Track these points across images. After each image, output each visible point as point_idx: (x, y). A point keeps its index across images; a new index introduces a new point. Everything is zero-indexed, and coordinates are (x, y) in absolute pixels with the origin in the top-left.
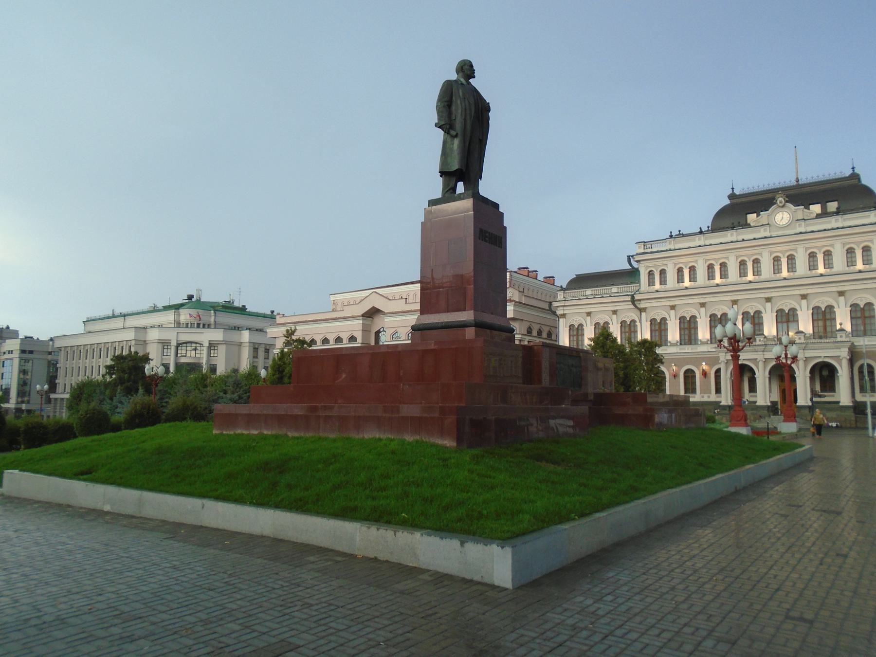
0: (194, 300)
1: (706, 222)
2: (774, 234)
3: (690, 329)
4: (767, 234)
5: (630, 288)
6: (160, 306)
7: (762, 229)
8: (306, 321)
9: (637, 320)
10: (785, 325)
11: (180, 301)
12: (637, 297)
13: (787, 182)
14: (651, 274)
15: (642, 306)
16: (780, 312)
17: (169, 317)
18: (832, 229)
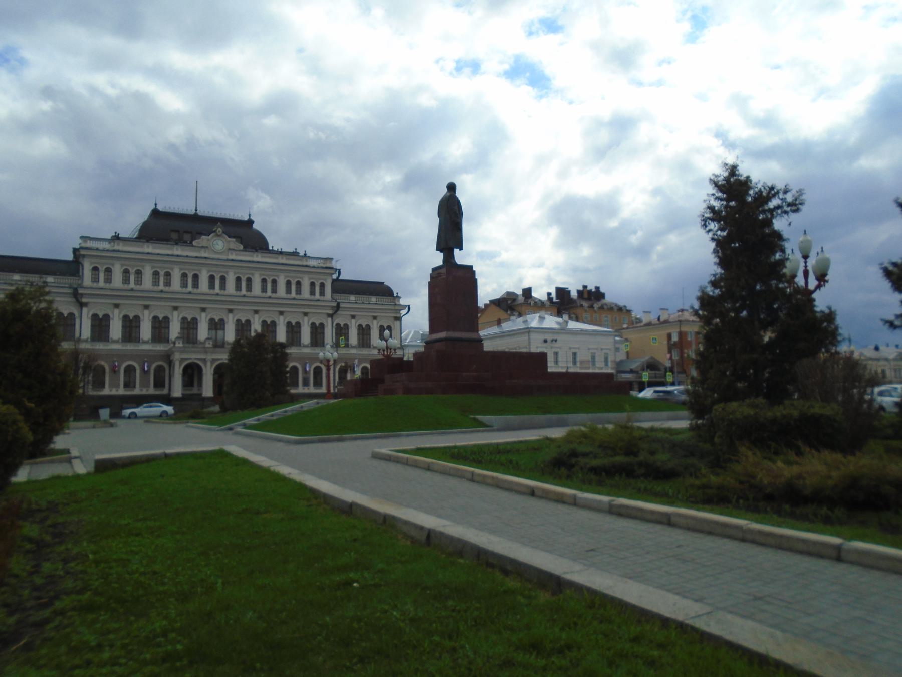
4: (206, 255)
7: (203, 250)
9: (77, 315)
10: (214, 332)
12: (81, 291)
15: (84, 300)
16: (212, 321)
18: (253, 262)
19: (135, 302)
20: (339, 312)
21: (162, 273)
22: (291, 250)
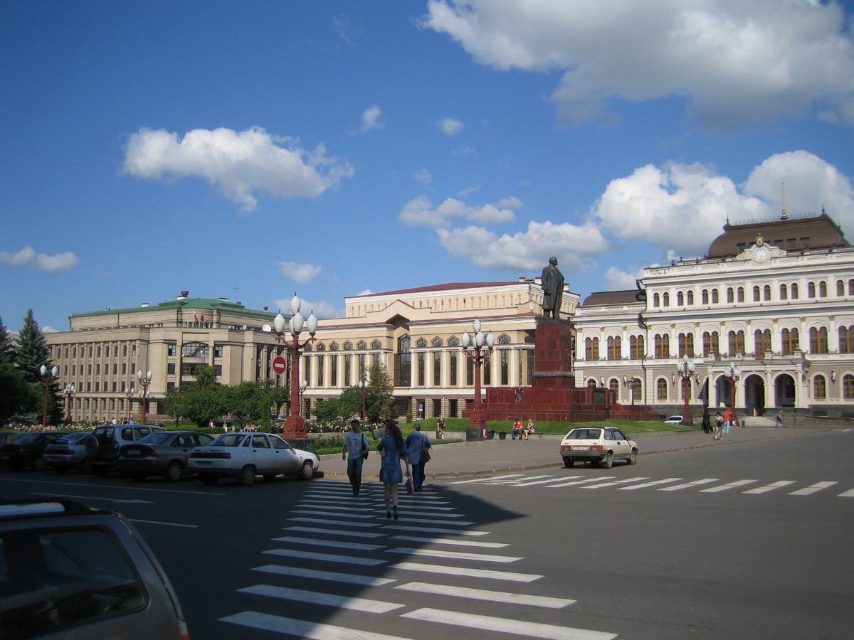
14: (656, 297)
15: (648, 323)
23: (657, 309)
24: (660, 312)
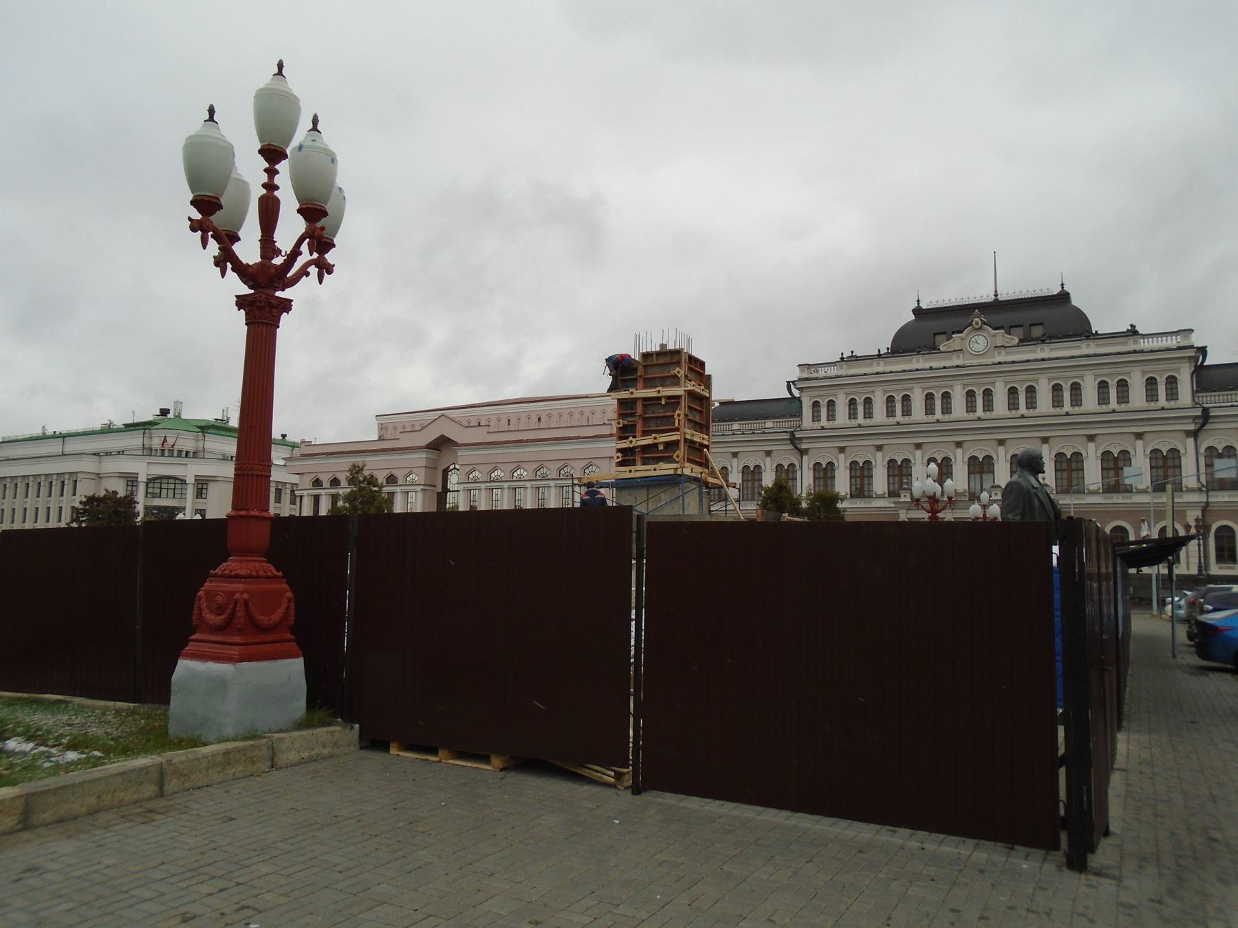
0: (171, 415)
1: (885, 345)
2: (968, 362)
3: (862, 477)
4: (960, 362)
5: (787, 424)
6: (119, 422)
8: (343, 453)
10: (978, 476)
11: (150, 418)
13: (985, 296)
15: (804, 446)
16: (973, 460)
17: (136, 440)
18: (1036, 360)
19: (1126, 430)
20: (1208, 426)
21: (898, 398)
22: (1124, 327)
23: (817, 425)
24: (823, 428)
